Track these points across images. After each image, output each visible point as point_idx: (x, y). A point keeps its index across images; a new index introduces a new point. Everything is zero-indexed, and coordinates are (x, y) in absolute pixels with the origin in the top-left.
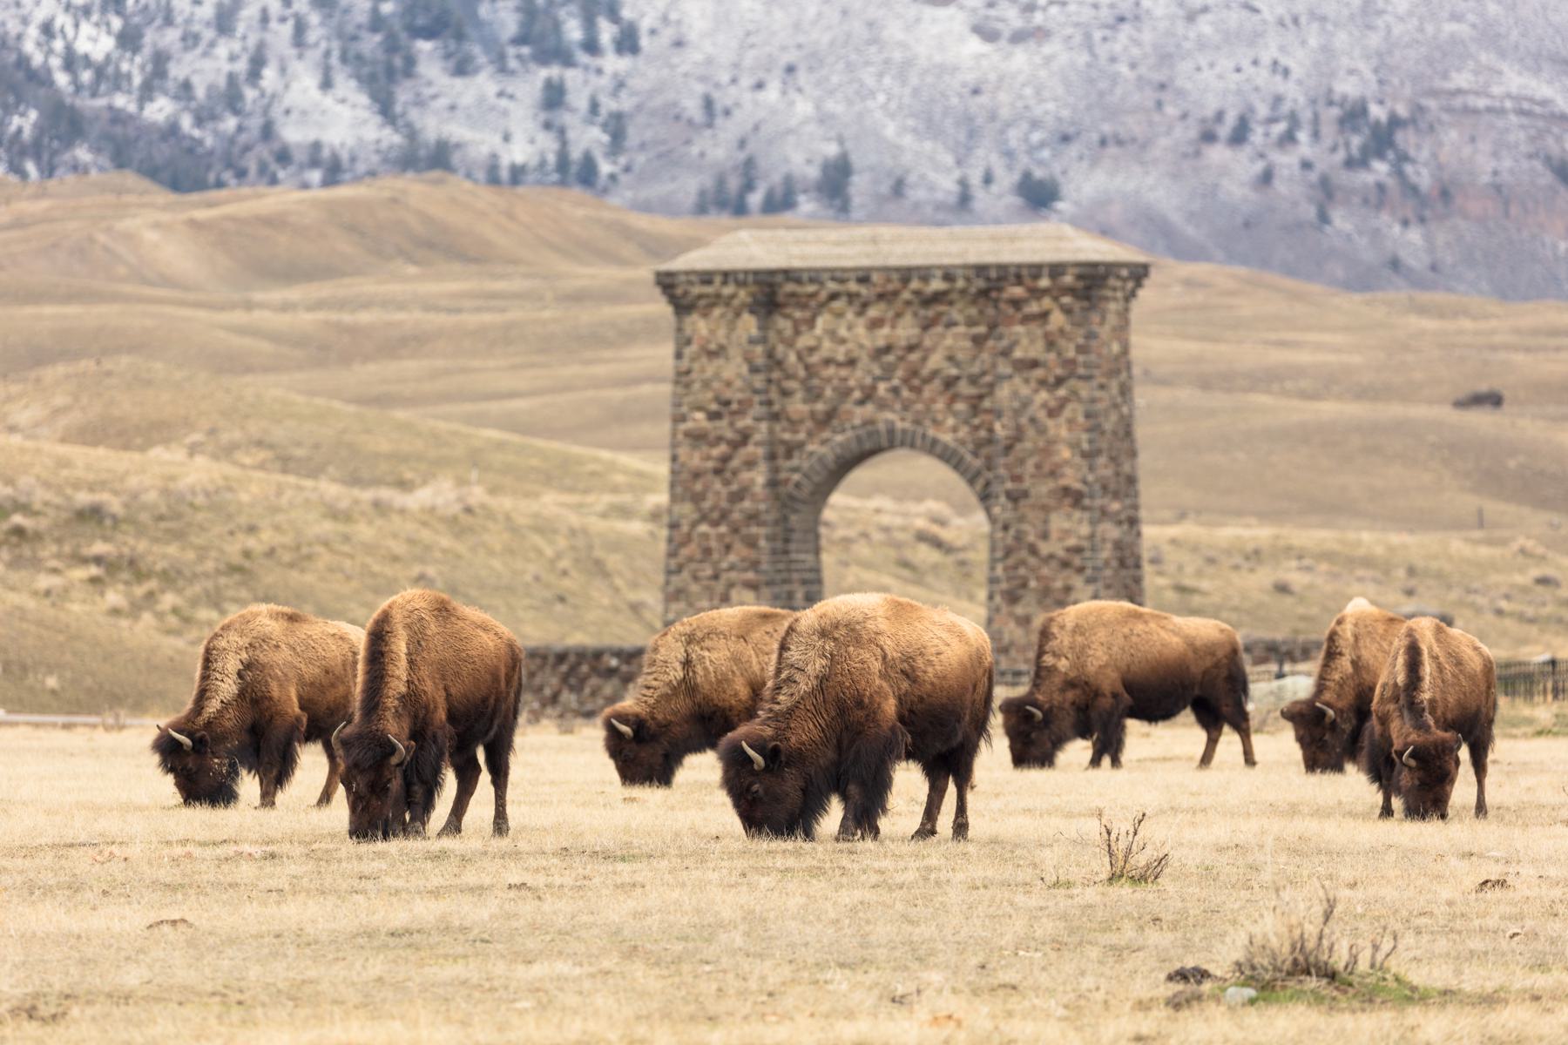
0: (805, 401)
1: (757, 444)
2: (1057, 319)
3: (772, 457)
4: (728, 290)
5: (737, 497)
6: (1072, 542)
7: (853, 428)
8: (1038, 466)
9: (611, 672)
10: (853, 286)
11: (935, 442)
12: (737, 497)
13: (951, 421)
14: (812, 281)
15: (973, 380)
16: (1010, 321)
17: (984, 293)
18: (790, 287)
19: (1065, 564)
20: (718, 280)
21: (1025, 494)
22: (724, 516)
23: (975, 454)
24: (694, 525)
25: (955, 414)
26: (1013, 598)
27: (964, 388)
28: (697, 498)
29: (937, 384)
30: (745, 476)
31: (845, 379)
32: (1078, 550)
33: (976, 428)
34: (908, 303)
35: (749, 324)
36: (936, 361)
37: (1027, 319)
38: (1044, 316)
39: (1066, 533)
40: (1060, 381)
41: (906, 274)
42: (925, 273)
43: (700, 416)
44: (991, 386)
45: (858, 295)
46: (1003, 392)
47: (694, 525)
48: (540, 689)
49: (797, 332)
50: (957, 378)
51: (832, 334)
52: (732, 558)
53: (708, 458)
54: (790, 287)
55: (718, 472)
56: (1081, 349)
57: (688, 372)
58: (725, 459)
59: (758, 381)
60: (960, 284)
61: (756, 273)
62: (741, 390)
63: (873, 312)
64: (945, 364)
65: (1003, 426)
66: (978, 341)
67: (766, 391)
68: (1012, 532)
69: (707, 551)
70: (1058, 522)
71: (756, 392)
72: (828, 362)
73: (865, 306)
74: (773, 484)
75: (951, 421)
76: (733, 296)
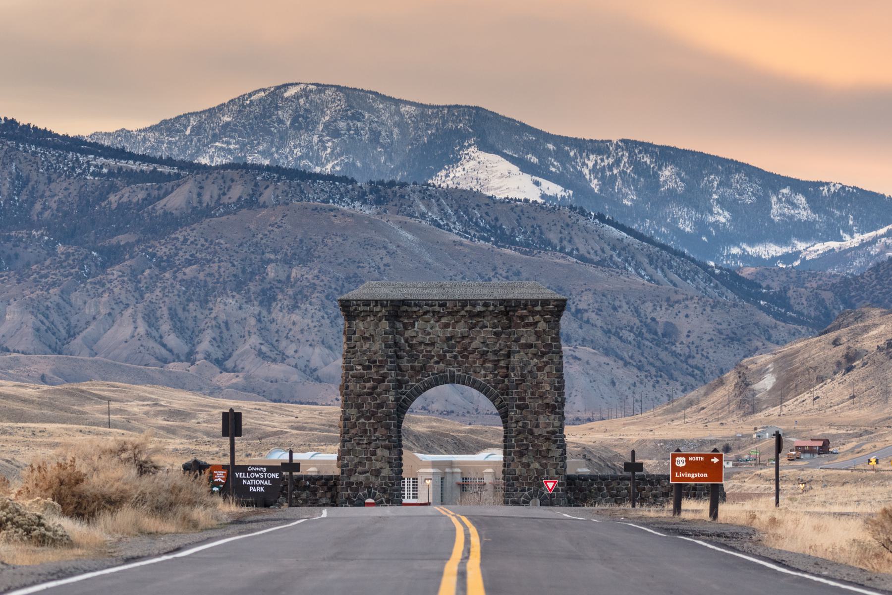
0: (408, 362)
2: (542, 326)
4: (376, 309)
5: (380, 406)
7: (433, 374)
8: (532, 394)
9: (306, 488)
10: (437, 308)
11: (475, 381)
12: (380, 406)
13: (483, 372)
14: (416, 305)
15: (495, 353)
16: (518, 326)
17: (506, 313)
18: (405, 308)
19: (548, 439)
20: (372, 304)
21: (527, 407)
22: (373, 414)
23: (495, 388)
24: (358, 418)
25: (485, 369)
26: (521, 455)
27: (491, 356)
28: (359, 407)
31: (430, 352)
32: (554, 433)
33: (496, 375)
34: (462, 316)
35: (385, 325)
36: (476, 344)
37: (527, 325)
38: (536, 324)
39: (548, 425)
40: (543, 354)
41: (464, 303)
42: (474, 303)
43: (359, 367)
44: (508, 356)
45: (439, 312)
46: (515, 359)
47: (358, 418)
49: (406, 328)
50: (488, 352)
51: (424, 330)
53: (365, 387)
54: (405, 308)
55: (370, 394)
56: (553, 339)
57: (354, 347)
58: (374, 388)
59: (390, 352)
60: (491, 308)
61: (392, 301)
62: (382, 356)
63: (444, 320)
64: (481, 345)
65: (515, 375)
66: (495, 333)
68: (520, 424)
71: (388, 357)
72: (420, 343)
73: (440, 318)
74: (397, 400)
75: (483, 372)
76: (378, 312)
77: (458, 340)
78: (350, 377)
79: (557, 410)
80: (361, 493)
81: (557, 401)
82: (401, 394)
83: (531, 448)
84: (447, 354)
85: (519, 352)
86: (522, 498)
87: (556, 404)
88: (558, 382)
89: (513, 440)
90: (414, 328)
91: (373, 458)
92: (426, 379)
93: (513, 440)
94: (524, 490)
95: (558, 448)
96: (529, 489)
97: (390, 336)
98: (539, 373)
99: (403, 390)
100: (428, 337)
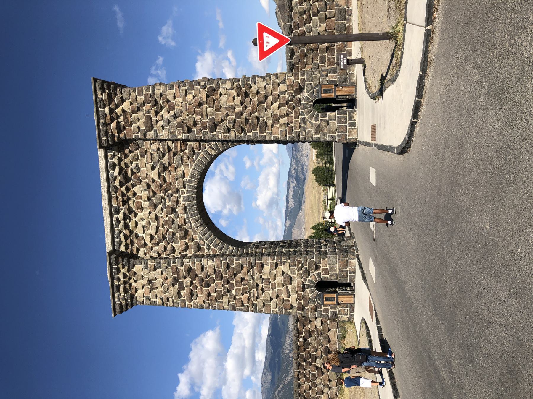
0: (178, 242)
1: (194, 264)
2: (126, 106)
6: (234, 92)
10: (120, 216)
14: (119, 237)
19: (246, 95)
26: (264, 127)
28: (221, 296)
29: (166, 175)
30: (209, 271)
31: (165, 221)
32: (239, 88)
34: (128, 189)
36: (154, 175)
45: (124, 214)
48: (314, 375)
52: (247, 278)
56: (140, 93)
58: (202, 281)
59: (164, 264)
63: (134, 207)
64: (156, 170)
65: (179, 134)
69: (245, 291)
73: (130, 211)
76: (125, 276)
77: (151, 194)
78: (192, 303)
79: (214, 85)
80: (310, 296)
82: (209, 249)
84: (167, 204)
85: (156, 131)
86: (313, 121)
87: (208, 86)
88: (184, 85)
90: (143, 237)
91: (272, 282)
92: (193, 225)
94: (303, 120)
95: (255, 83)
96: (302, 114)
97: (149, 263)
98: (176, 108)
100: (152, 223)
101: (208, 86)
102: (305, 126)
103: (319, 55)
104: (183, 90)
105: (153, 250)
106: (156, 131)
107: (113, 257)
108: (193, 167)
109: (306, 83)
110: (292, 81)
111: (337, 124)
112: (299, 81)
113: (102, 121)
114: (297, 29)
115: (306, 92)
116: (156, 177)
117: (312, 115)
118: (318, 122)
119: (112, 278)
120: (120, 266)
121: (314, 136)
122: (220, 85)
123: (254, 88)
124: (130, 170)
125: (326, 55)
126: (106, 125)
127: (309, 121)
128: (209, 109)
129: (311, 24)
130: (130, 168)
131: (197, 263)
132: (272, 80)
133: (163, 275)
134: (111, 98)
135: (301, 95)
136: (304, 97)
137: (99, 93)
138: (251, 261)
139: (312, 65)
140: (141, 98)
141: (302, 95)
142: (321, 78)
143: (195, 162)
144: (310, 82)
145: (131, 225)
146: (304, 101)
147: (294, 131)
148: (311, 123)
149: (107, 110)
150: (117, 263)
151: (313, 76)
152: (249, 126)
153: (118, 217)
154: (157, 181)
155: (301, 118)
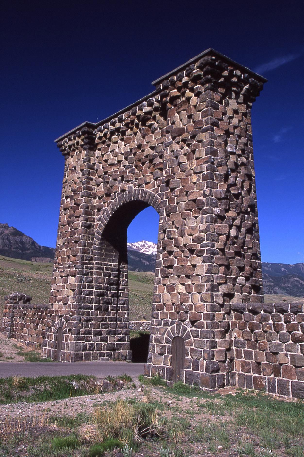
3: (86, 213)
36: (148, 151)
39: (193, 229)
45: (120, 128)
67: (89, 183)
70: (191, 223)
76: (78, 143)
81: (205, 196)
83: (176, 265)
87: (204, 199)
89: (161, 255)
92: (113, 201)
93: (161, 255)
94: (166, 324)
95: (204, 262)
99: (100, 216)
101: (204, 199)
102: (162, 326)
103: (253, 351)
104: (201, 168)
105: (100, 165)
106: (170, 143)
107: (85, 129)
108: (152, 193)
109: (199, 330)
110: (202, 310)
111: (159, 366)
112: (202, 320)
113: (175, 78)
114: (284, 319)
115: (192, 329)
116: (145, 154)
117: (170, 335)
118: (164, 342)
119: (74, 133)
120: (83, 137)
121: (154, 336)
122: (205, 216)
123: (198, 261)
124: (151, 123)
125: (253, 361)
126: (173, 84)
127: (165, 331)
128: (184, 203)
129: (291, 342)
130: (153, 122)
131: (82, 210)
132: (206, 284)
133: (77, 179)
134: (196, 80)
135: (188, 322)
136: (186, 325)
137: (197, 64)
138: (78, 265)
139: (242, 339)
140: (199, 116)
141: (189, 323)
142: (203, 350)
143: (156, 195)
144: (200, 335)
145: (114, 137)
146: (183, 326)
147: (159, 312)
148: (164, 334)
149: (185, 79)
150: (84, 133)
151: (206, 340)
152: (166, 256)
153: (116, 123)
154: (143, 155)
155: (169, 320)
